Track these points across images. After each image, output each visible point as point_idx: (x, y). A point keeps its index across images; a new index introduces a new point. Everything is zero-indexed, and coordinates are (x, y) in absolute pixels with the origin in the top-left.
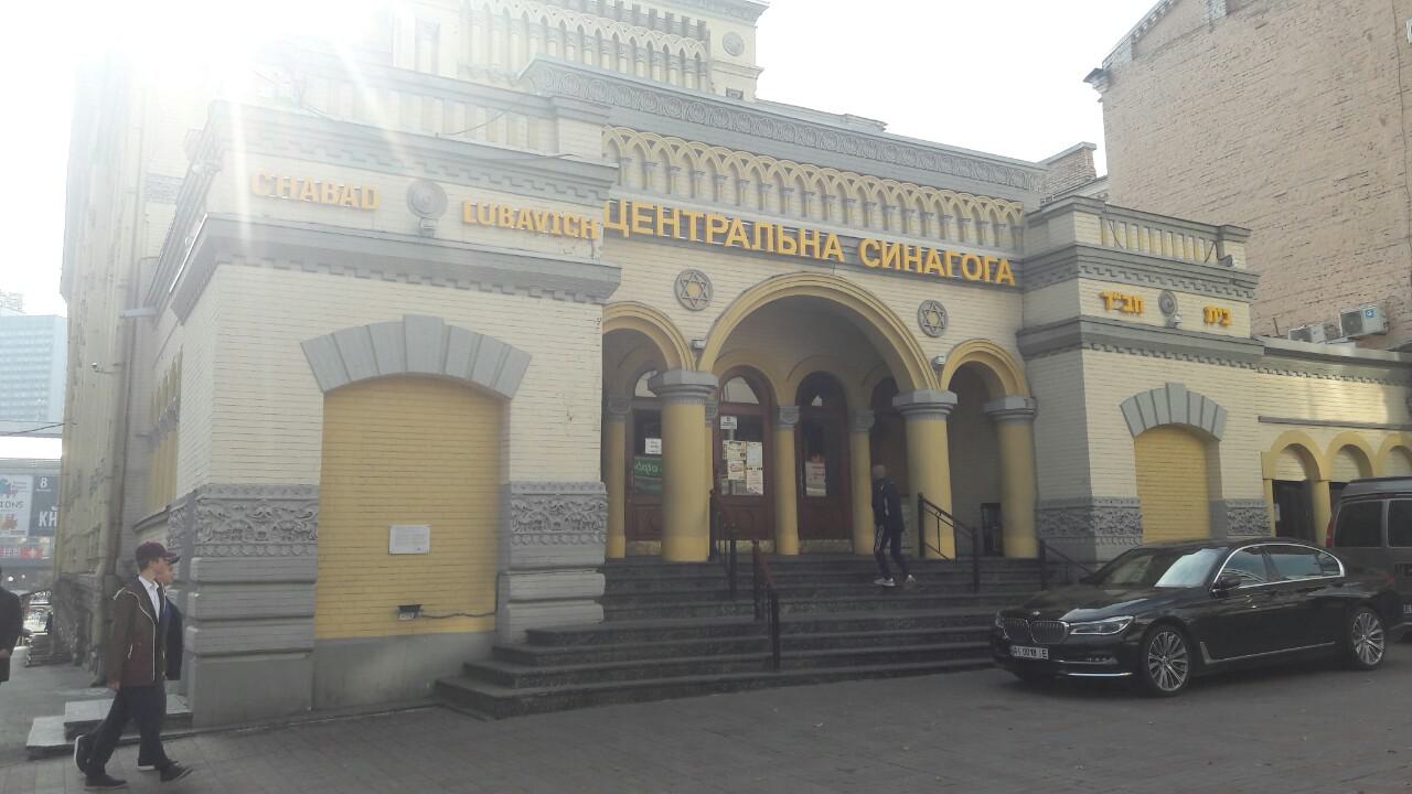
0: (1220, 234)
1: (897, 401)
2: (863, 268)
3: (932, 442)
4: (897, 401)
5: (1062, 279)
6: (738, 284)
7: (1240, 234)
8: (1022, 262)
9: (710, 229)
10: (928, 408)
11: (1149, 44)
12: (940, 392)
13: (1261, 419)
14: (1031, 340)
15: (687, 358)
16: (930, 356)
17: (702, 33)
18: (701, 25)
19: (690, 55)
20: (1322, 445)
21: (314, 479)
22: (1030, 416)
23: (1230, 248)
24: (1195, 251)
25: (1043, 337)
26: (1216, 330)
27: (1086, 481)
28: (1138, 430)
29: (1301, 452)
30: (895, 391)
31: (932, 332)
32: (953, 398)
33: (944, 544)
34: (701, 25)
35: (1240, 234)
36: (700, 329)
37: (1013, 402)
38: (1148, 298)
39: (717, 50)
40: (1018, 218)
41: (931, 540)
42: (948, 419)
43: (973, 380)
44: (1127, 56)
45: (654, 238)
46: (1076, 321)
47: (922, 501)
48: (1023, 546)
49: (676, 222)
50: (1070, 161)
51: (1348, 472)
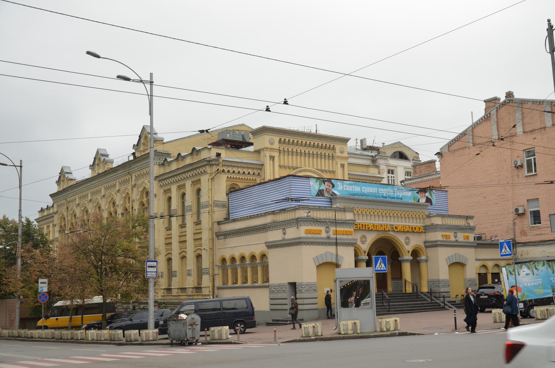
0: (467, 218)
1: (400, 259)
2: (394, 231)
3: (407, 269)
4: (400, 259)
5: (434, 231)
6: (371, 238)
7: (471, 218)
8: (425, 226)
9: (367, 227)
10: (407, 260)
11: (453, 148)
12: (409, 257)
13: (477, 260)
14: (427, 244)
15: (363, 253)
16: (407, 249)
17: (334, 149)
18: (334, 146)
19: (331, 155)
20: (490, 264)
21: (316, 281)
22: (426, 261)
23: (470, 221)
24: (461, 222)
25: (430, 244)
26: (466, 240)
27: (438, 275)
28: (449, 264)
29: (484, 266)
30: (399, 256)
31: (407, 244)
32: (411, 258)
33: (409, 289)
34: (334, 146)
35: (471, 218)
36: (365, 247)
37: (423, 258)
38: (451, 234)
39: (338, 154)
40: (424, 217)
41: (407, 289)
42: (411, 263)
43: (415, 253)
44: (446, 150)
45: (357, 230)
46: (437, 241)
47: (405, 281)
48: (425, 289)
49: (361, 226)
50: (428, 165)
51: (496, 271)
